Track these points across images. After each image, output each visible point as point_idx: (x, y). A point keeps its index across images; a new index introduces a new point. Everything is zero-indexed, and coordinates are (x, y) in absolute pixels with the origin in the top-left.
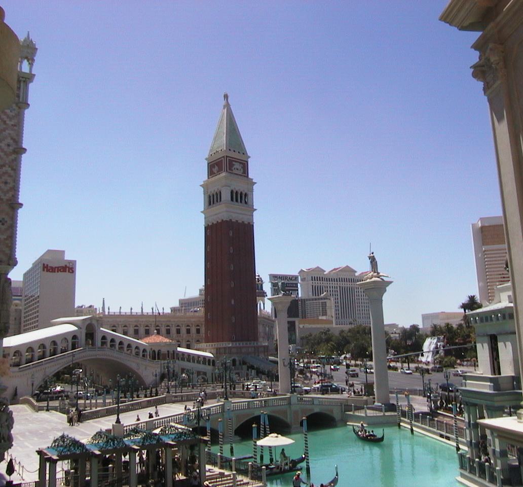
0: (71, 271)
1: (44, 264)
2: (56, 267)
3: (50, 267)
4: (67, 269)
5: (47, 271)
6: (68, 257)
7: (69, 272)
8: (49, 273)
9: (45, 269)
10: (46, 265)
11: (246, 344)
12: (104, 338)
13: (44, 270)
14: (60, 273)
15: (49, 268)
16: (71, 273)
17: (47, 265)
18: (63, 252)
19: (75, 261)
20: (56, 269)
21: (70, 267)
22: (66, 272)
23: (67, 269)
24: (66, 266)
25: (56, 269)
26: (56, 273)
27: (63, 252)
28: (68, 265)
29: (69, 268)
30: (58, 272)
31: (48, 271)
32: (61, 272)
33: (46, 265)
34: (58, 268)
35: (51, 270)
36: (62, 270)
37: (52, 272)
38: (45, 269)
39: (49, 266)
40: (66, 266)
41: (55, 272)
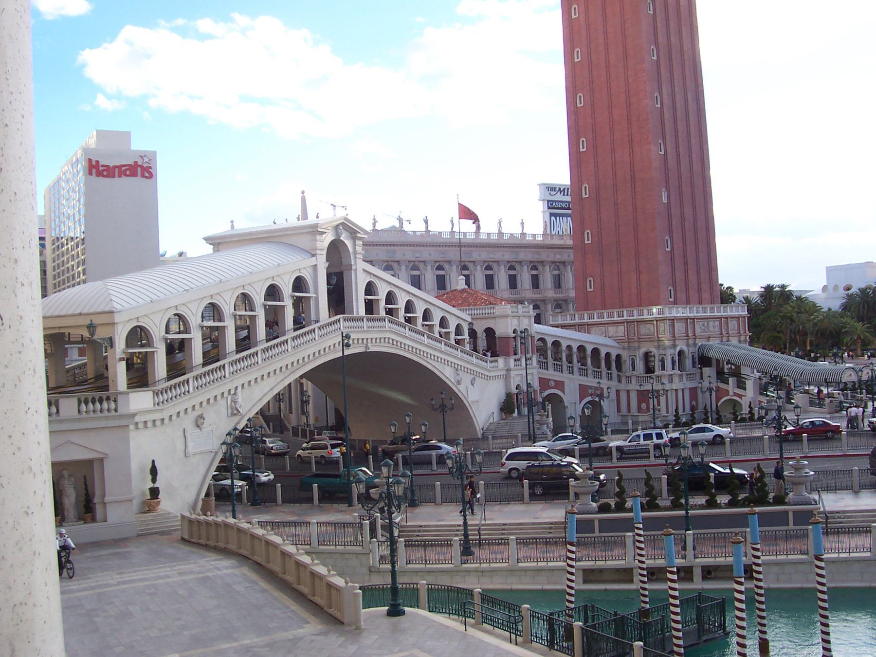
0: (147, 174)
1: (90, 160)
3: (103, 166)
4: (139, 169)
5: (98, 175)
6: (139, 144)
7: (143, 176)
8: (101, 179)
9: (94, 171)
10: (94, 163)
11: (610, 315)
12: (370, 289)
13: (90, 174)
14: (124, 178)
16: (147, 177)
17: (97, 162)
18: (127, 135)
19: (155, 153)
20: (117, 170)
21: (145, 165)
22: (136, 175)
23: (139, 169)
24: (136, 162)
25: (117, 170)
26: (117, 179)
27: (127, 135)
28: (140, 163)
29: (141, 166)
30: (120, 176)
31: (99, 174)
32: (126, 175)
33: (94, 163)
37: (108, 176)
38: (94, 171)
39: (101, 164)
40: (136, 162)
41: (114, 177)
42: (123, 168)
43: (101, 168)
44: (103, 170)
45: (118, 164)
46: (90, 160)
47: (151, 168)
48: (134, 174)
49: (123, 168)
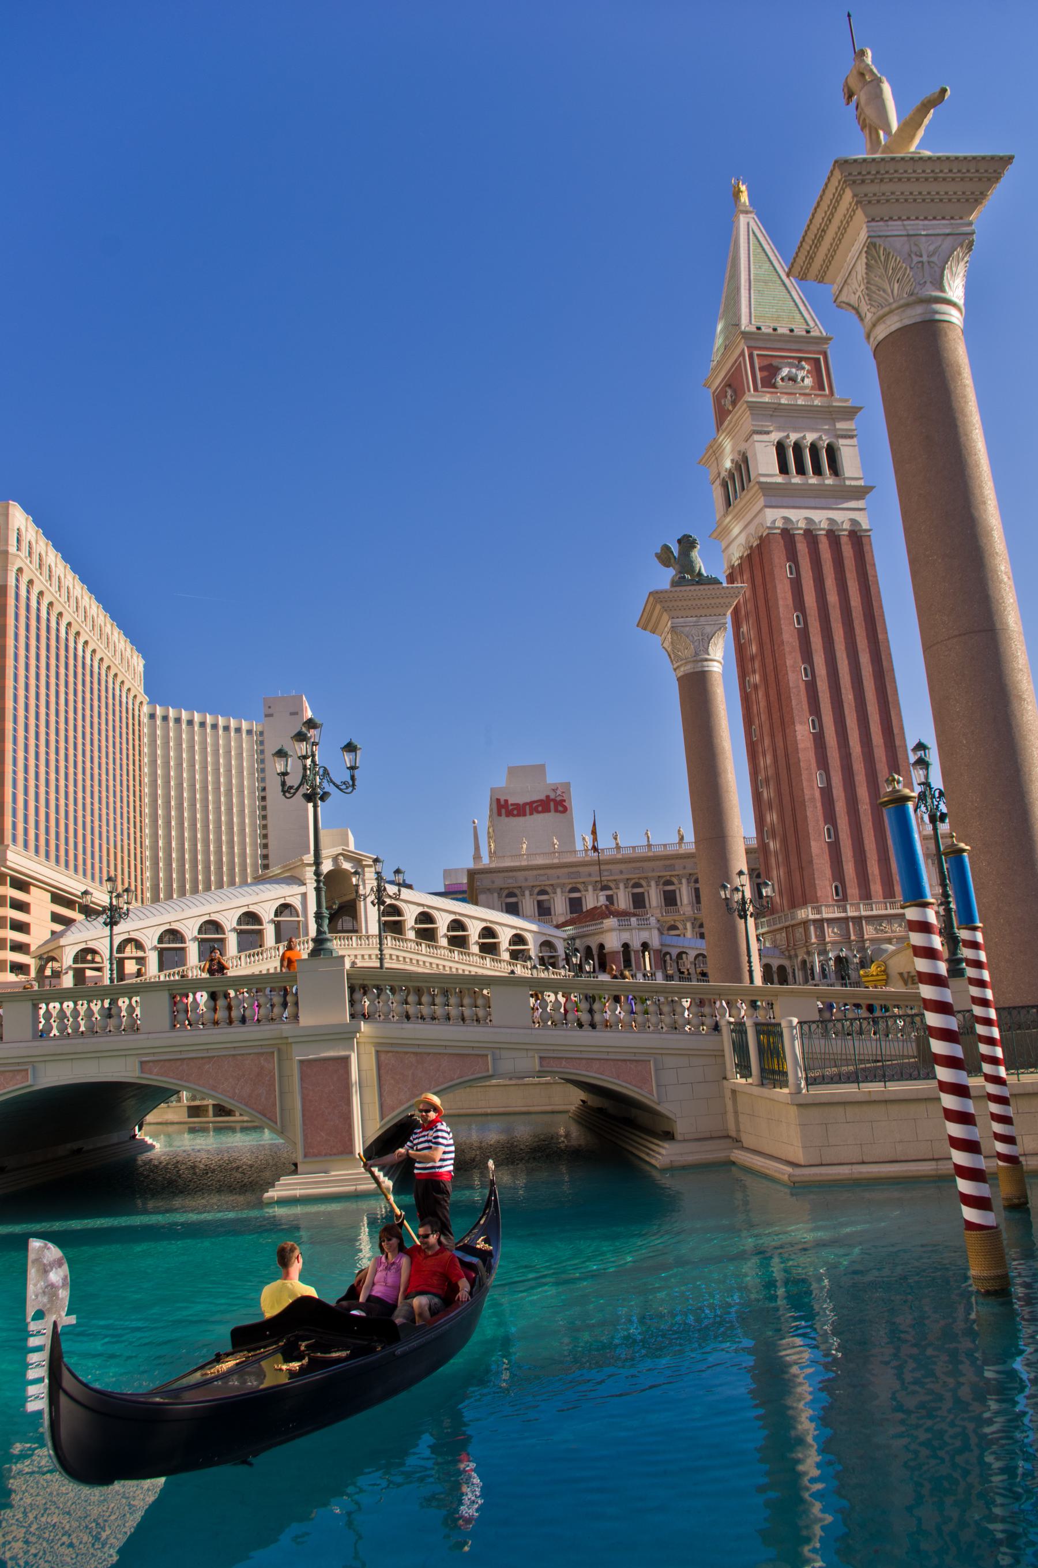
0: (560, 808)
1: (498, 800)
2: (525, 804)
3: (512, 805)
4: (552, 804)
6: (553, 777)
7: (556, 811)
9: (503, 811)
10: (502, 802)
15: (510, 808)
17: (506, 801)
20: (528, 807)
22: (549, 811)
23: (552, 804)
24: (548, 797)
25: (528, 807)
26: (528, 817)
28: (552, 796)
29: (554, 800)
30: (531, 814)
31: (509, 814)
32: (538, 812)
33: (502, 802)
34: (531, 803)
35: (515, 812)
36: (540, 809)
38: (503, 811)
39: (510, 803)
42: (534, 805)
43: (510, 808)
44: (513, 810)
45: (528, 800)
46: (498, 800)
47: (564, 801)
48: (546, 810)
49: (534, 805)
